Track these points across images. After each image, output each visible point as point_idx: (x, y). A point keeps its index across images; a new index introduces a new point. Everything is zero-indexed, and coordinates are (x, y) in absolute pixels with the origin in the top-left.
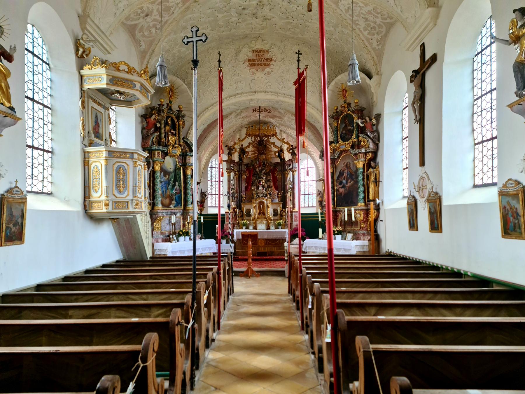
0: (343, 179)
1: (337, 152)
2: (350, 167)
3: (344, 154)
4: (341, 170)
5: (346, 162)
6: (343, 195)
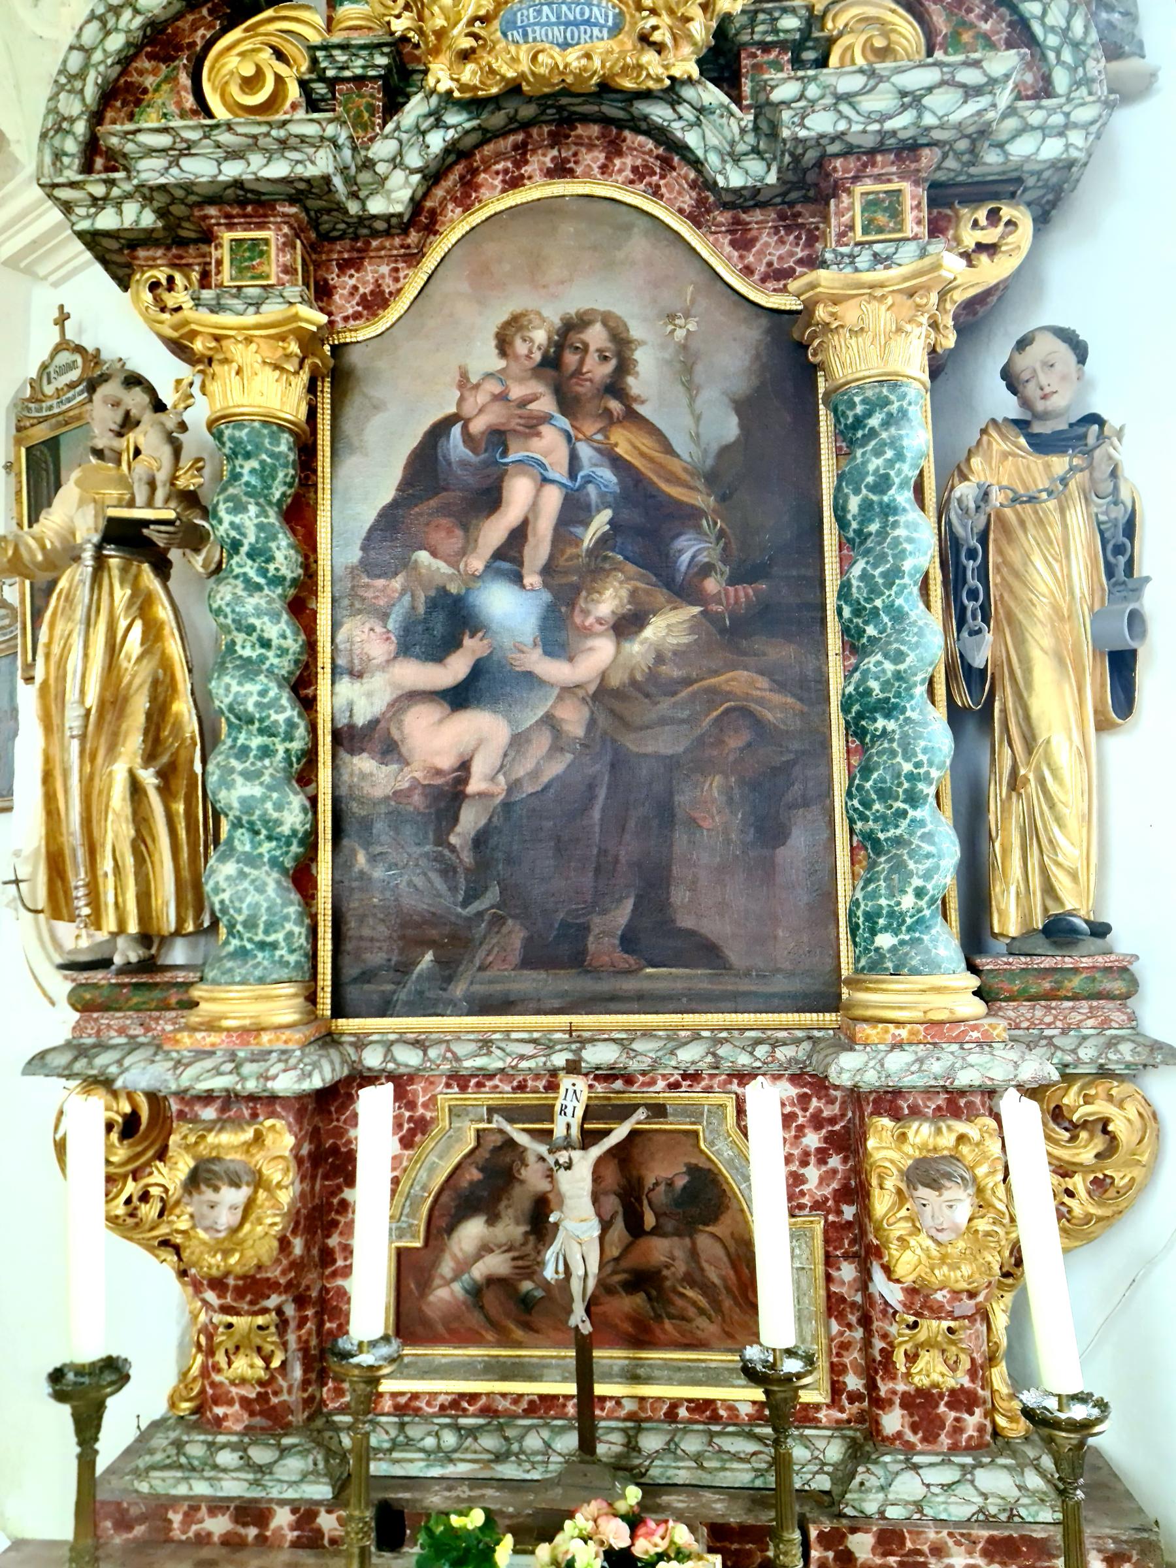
0: (477, 564)
1: (415, 108)
2: (615, 387)
3: (514, 183)
4: (440, 429)
5: (554, 314)
6: (470, 820)
